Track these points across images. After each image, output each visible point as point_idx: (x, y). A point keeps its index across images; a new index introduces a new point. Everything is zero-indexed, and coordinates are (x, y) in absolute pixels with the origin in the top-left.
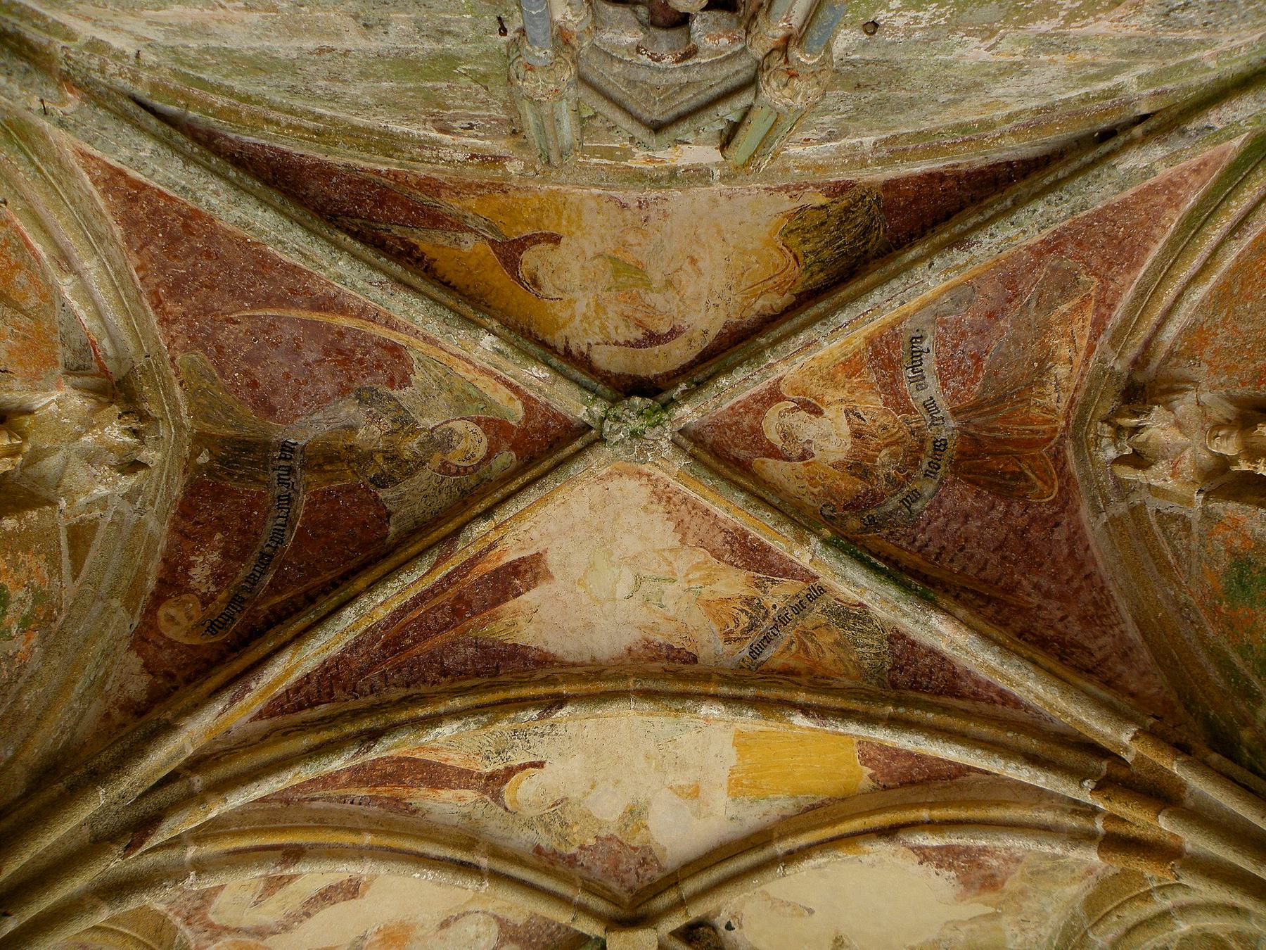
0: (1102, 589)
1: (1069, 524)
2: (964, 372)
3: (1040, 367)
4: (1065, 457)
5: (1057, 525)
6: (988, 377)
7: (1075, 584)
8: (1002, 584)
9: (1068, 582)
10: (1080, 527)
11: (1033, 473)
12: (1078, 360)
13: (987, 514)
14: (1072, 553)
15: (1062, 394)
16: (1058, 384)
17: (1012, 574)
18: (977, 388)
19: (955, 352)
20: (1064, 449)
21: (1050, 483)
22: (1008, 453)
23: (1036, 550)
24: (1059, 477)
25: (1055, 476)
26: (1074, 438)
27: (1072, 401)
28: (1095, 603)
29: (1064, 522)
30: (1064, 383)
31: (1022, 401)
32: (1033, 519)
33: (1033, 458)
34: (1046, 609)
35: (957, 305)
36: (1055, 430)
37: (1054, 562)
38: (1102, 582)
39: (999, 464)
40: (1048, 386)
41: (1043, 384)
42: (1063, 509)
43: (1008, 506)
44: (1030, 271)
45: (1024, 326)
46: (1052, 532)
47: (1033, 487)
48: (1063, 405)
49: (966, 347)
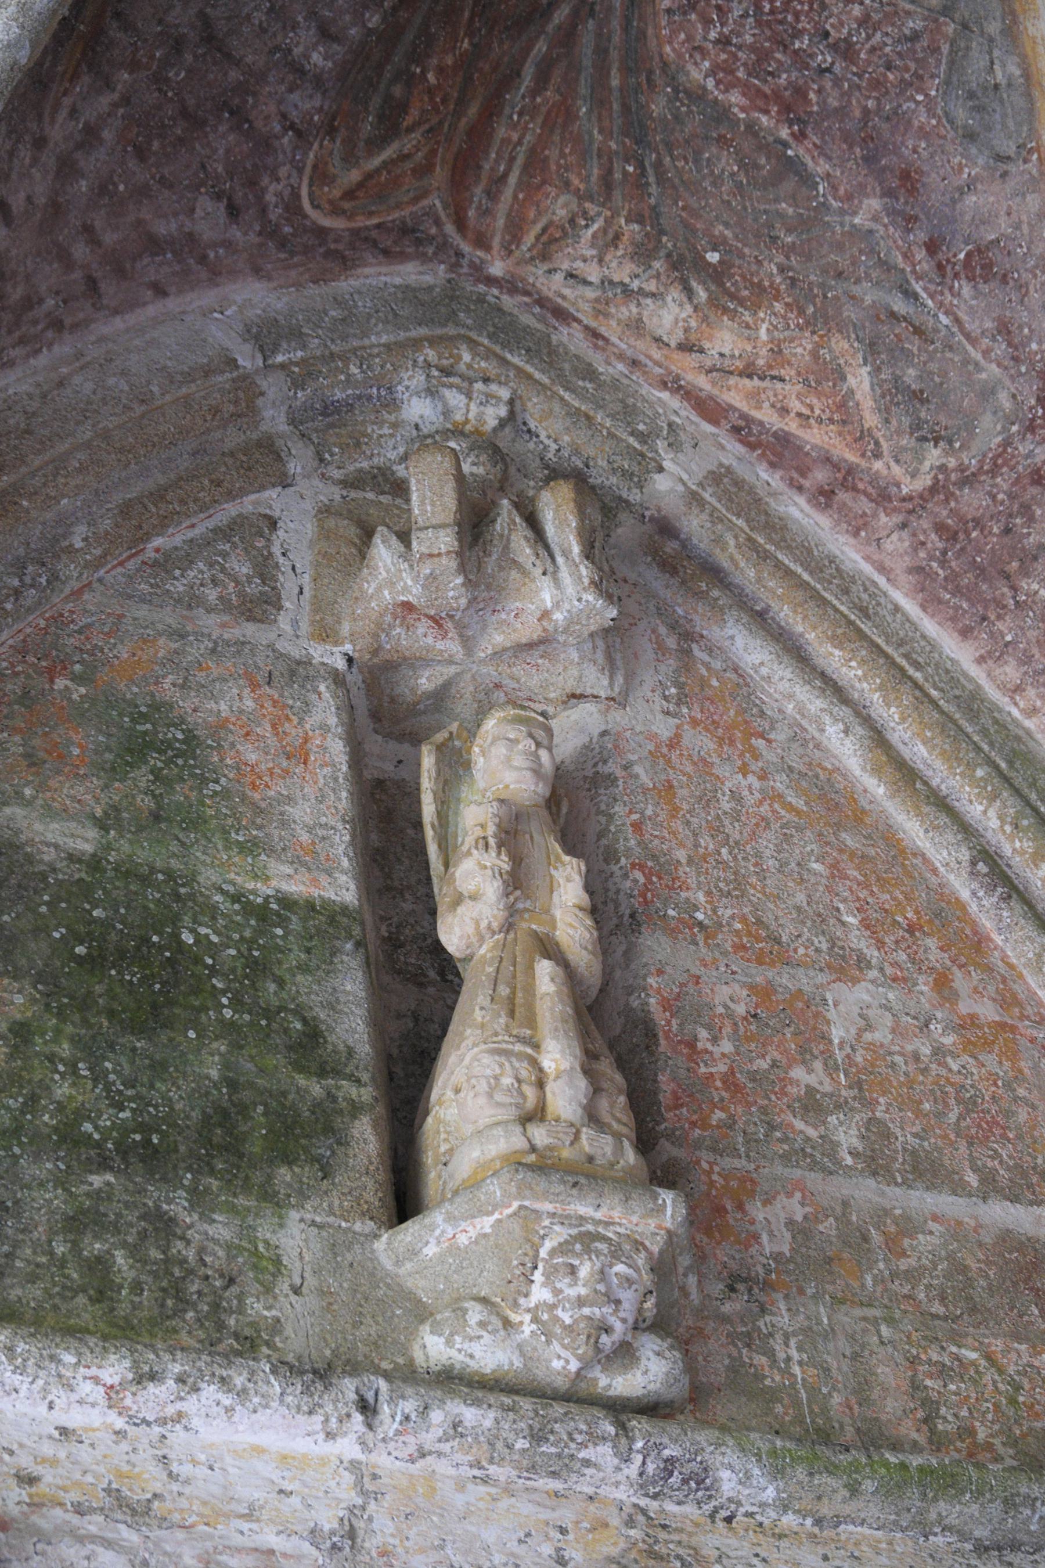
0: (57, 325)
1: (228, 244)
2: (763, 56)
3: (700, 265)
4: (403, 257)
5: (233, 212)
6: (722, 114)
7: (80, 251)
8: (115, 32)
9: (88, 229)
10: (216, 274)
11: (385, 163)
12: (687, 367)
13: (312, 14)
14: (154, 245)
15: (590, 294)
16: (628, 293)
17: (134, 66)
18: (697, 73)
19: (834, 47)
20: (424, 258)
21: (347, 205)
22: (462, 103)
23: (181, 140)
24: (355, 232)
25: (361, 222)
26: (451, 293)
27: (562, 315)
28: (29, 303)
29: (236, 233)
30: (628, 311)
31: (607, 183)
32: (265, 144)
33: (425, 170)
34: (35, 161)
35: (971, 95)
36: (482, 242)
37: (142, 192)
38: (75, 327)
39: (441, 70)
40: (629, 267)
41: (642, 254)
42: (270, 232)
43: (318, 81)
44: (1004, 328)
45: (843, 261)
46: (218, 197)
47: (349, 159)
48: (554, 286)
49: (837, 82)
